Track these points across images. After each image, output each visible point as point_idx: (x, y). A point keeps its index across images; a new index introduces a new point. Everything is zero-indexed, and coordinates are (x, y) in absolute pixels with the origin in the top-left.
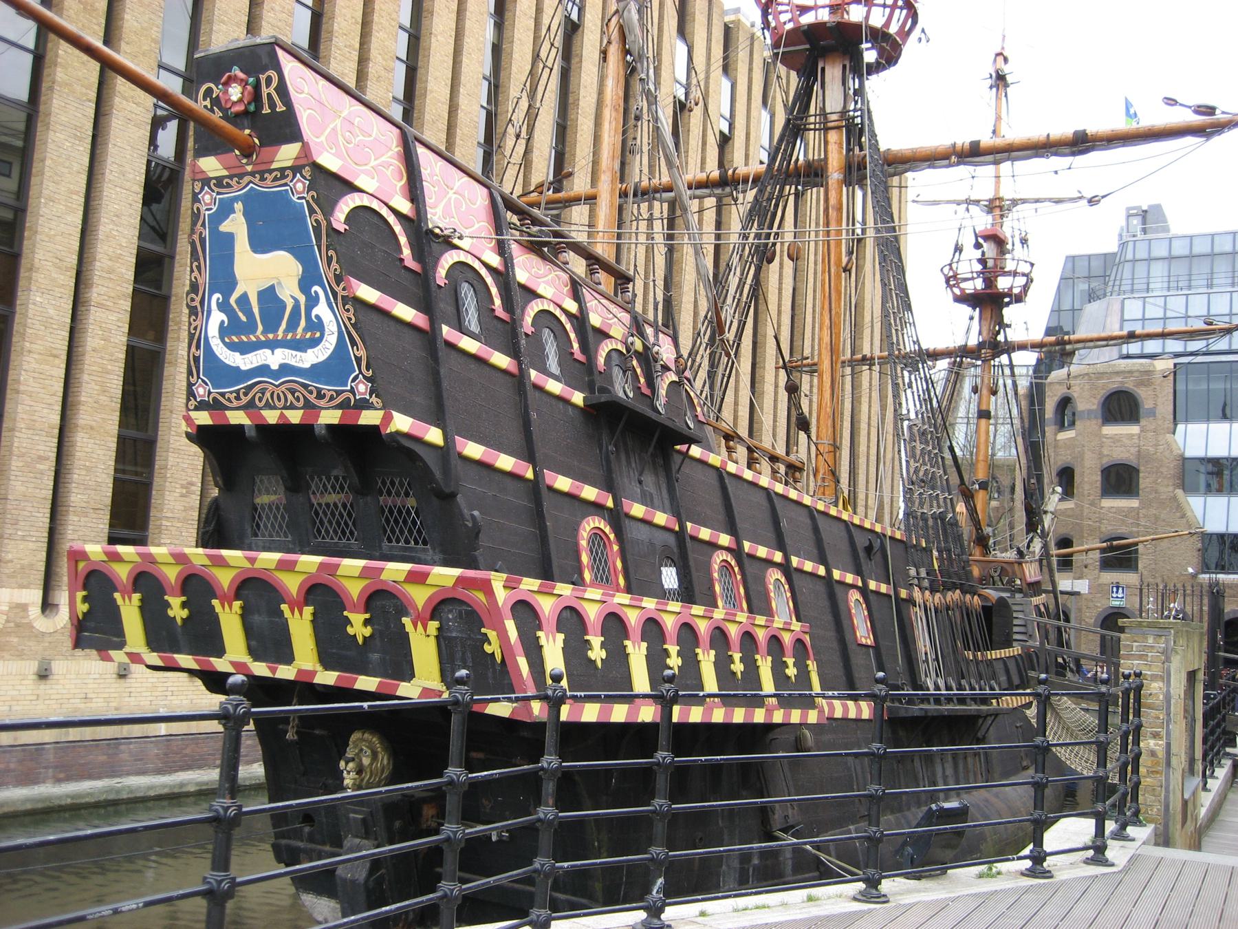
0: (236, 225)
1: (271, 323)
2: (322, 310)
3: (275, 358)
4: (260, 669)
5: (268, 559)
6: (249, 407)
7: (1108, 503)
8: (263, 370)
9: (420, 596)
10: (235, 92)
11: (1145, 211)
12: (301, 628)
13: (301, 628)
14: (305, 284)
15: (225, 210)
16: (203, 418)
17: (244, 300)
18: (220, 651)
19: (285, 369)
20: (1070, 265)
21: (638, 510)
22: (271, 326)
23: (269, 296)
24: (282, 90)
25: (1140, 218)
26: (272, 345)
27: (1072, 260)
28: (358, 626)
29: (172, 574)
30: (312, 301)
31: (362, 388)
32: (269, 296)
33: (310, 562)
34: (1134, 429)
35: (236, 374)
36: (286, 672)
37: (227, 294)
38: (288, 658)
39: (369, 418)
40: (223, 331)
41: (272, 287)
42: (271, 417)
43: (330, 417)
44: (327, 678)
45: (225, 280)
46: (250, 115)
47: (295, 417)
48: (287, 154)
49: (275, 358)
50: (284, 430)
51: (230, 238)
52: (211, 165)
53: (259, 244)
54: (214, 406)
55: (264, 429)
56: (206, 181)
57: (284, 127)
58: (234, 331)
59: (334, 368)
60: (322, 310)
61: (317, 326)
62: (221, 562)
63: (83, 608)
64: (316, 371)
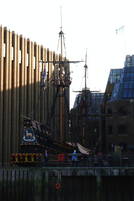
0: (27, 131)
2: (34, 137)
4: (29, 162)
5: (30, 154)
6: (27, 143)
7: (120, 135)
8: (29, 141)
11: (131, 57)
12: (32, 159)
13: (32, 159)
16: (22, 144)
20: (112, 72)
21: (51, 149)
24: (32, 123)
25: (130, 58)
27: (112, 71)
29: (21, 156)
32: (29, 136)
34: (126, 117)
35: (26, 141)
36: (31, 162)
37: (26, 136)
38: (31, 161)
39: (37, 144)
40: (25, 138)
41: (29, 136)
45: (25, 135)
46: (29, 124)
47: (31, 144)
48: (32, 127)
51: (26, 132)
53: (29, 133)
56: (24, 128)
57: (32, 125)
58: (26, 138)
59: (35, 141)
60: (34, 137)
61: (33, 138)
64: (33, 141)
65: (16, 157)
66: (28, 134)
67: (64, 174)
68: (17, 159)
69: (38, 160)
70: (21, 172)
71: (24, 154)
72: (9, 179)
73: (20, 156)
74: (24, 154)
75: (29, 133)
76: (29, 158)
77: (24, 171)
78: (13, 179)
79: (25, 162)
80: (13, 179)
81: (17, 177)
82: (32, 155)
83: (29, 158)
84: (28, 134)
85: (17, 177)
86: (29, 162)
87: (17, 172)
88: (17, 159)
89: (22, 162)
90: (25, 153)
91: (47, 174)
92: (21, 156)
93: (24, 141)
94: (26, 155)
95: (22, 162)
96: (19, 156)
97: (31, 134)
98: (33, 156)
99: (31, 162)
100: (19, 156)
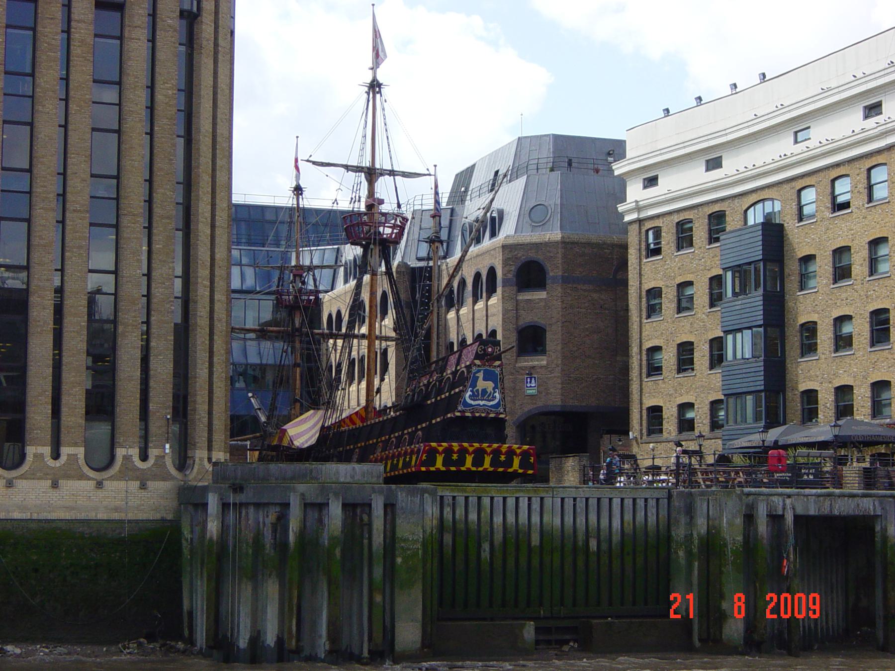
0: (481, 375)
1: (483, 395)
2: (497, 395)
3: (482, 403)
4: (474, 469)
8: (479, 405)
9: (518, 451)
10: (490, 350)
14: (494, 389)
15: (479, 371)
16: (458, 414)
17: (478, 390)
18: (464, 465)
19: (484, 405)
22: (483, 395)
23: (484, 391)
26: (482, 400)
28: (503, 458)
29: (456, 449)
30: (495, 392)
31: (502, 410)
33: (495, 446)
35: (471, 405)
36: (480, 469)
38: (482, 465)
40: (470, 396)
42: (477, 415)
43: (492, 415)
44: (492, 469)
45: (474, 385)
47: (483, 415)
48: (497, 363)
49: (482, 403)
50: (480, 417)
52: (477, 362)
53: (484, 379)
54: (463, 412)
55: (474, 417)
56: (475, 365)
59: (498, 405)
60: (497, 395)
62: (471, 446)
63: (424, 458)
64: (492, 406)
65: (440, 454)
66: (481, 384)
67: (800, 511)
68: (440, 460)
69: (502, 464)
70: (638, 501)
71: (465, 445)
72: (604, 522)
73: (453, 452)
74: (465, 445)
75: (484, 379)
76: (479, 457)
77: (646, 500)
78: (616, 523)
79: (463, 469)
80: (616, 523)
81: (628, 517)
82: (489, 450)
83: (479, 457)
84: (481, 384)
85: (628, 517)
86: (474, 469)
87: (626, 501)
88: (440, 460)
89: (453, 469)
90: (470, 441)
91: (762, 511)
92: (456, 449)
93: (466, 404)
94: (440, 449)
95: (453, 469)
96: (448, 451)
97: (489, 385)
98: (493, 452)
99: (480, 469)
100: (448, 451)
